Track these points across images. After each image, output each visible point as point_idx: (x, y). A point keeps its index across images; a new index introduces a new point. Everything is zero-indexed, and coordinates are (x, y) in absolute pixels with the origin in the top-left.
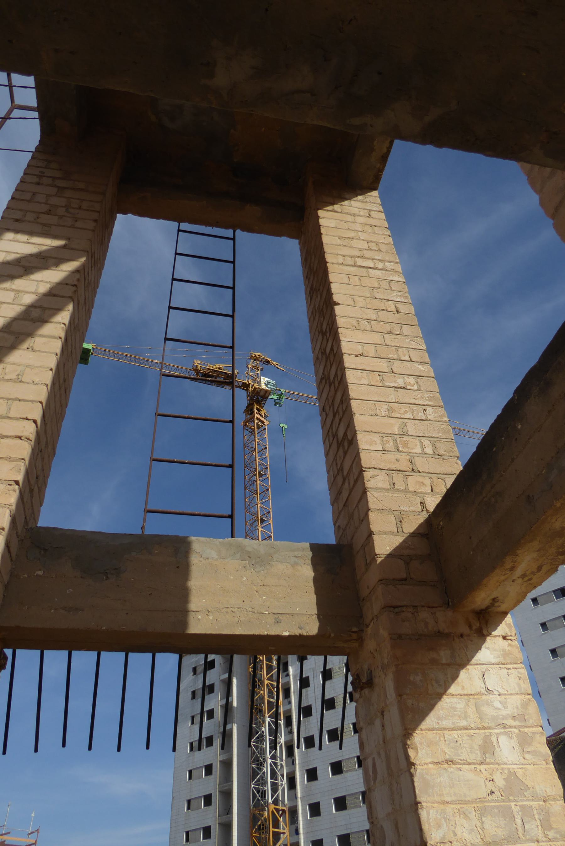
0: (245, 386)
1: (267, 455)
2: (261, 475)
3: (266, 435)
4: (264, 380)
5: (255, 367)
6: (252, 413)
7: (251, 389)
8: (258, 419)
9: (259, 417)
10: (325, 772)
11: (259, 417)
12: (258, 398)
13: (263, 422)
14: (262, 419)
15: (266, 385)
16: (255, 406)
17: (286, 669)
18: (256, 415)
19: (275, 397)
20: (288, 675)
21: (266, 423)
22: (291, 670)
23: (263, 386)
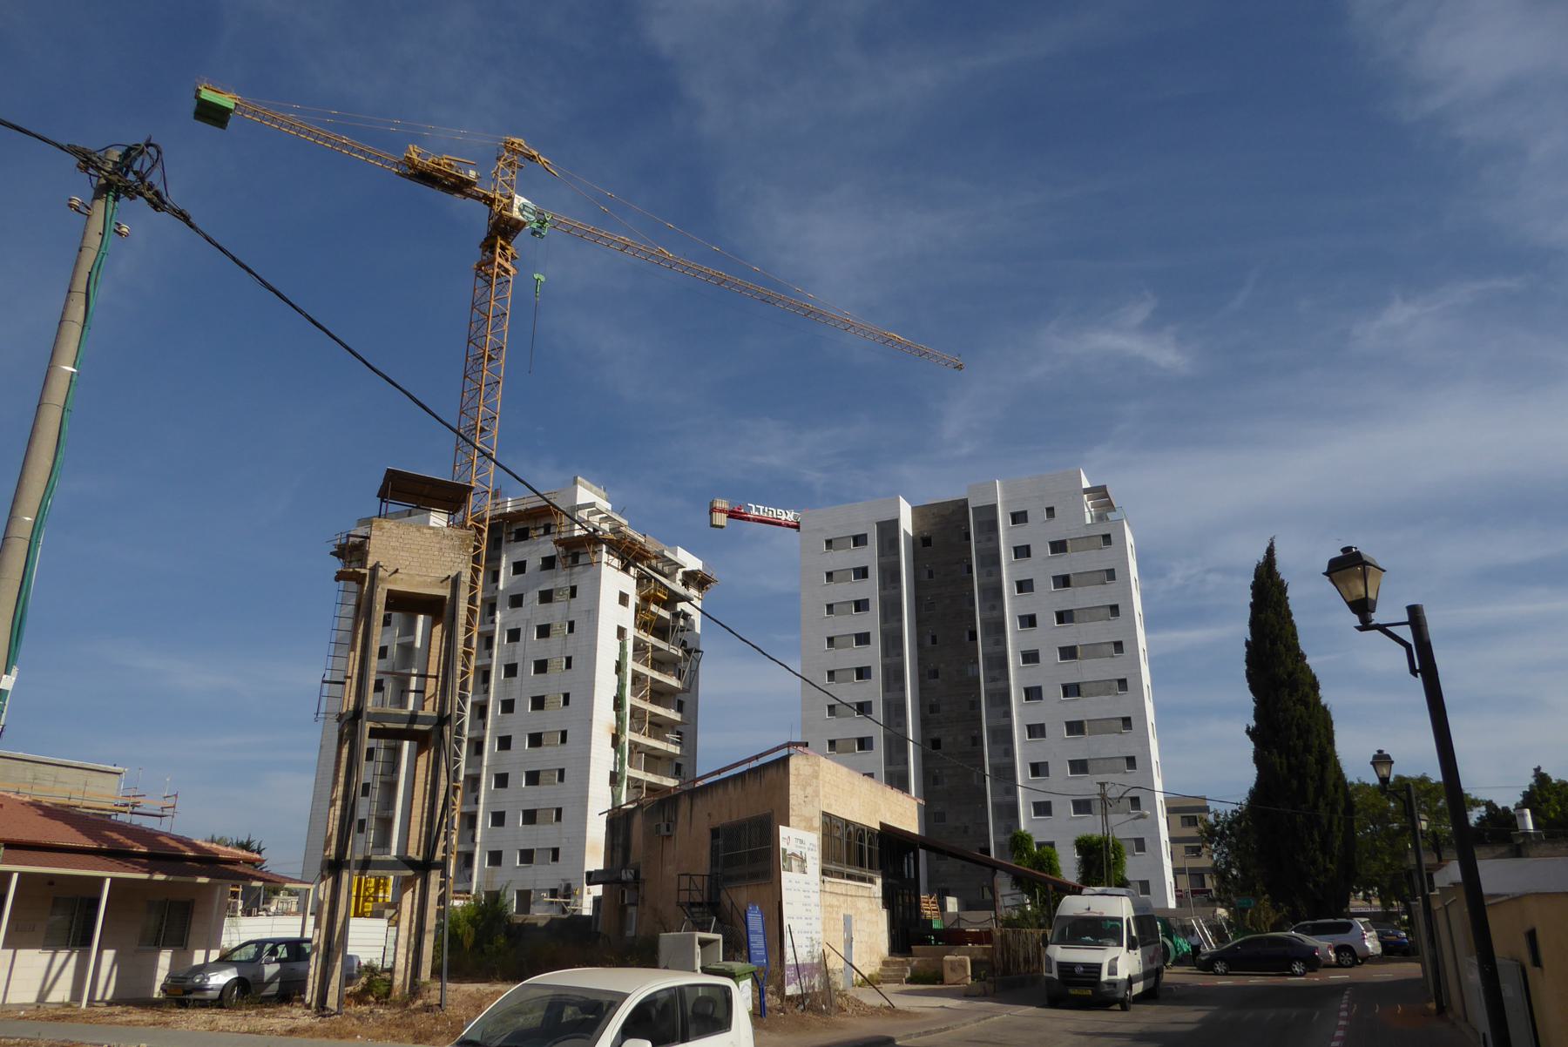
0: (490, 201)
1: (505, 327)
2: (490, 359)
3: (509, 294)
4: (519, 200)
5: (510, 164)
6: (493, 252)
7: (496, 208)
8: (500, 266)
9: (502, 262)
10: (521, 744)
11: (502, 262)
12: (505, 228)
13: (507, 271)
14: (507, 265)
15: (521, 211)
16: (500, 241)
17: (492, 613)
18: (498, 260)
19: (534, 226)
20: (493, 622)
21: (512, 271)
22: (498, 614)
23: (516, 214)
